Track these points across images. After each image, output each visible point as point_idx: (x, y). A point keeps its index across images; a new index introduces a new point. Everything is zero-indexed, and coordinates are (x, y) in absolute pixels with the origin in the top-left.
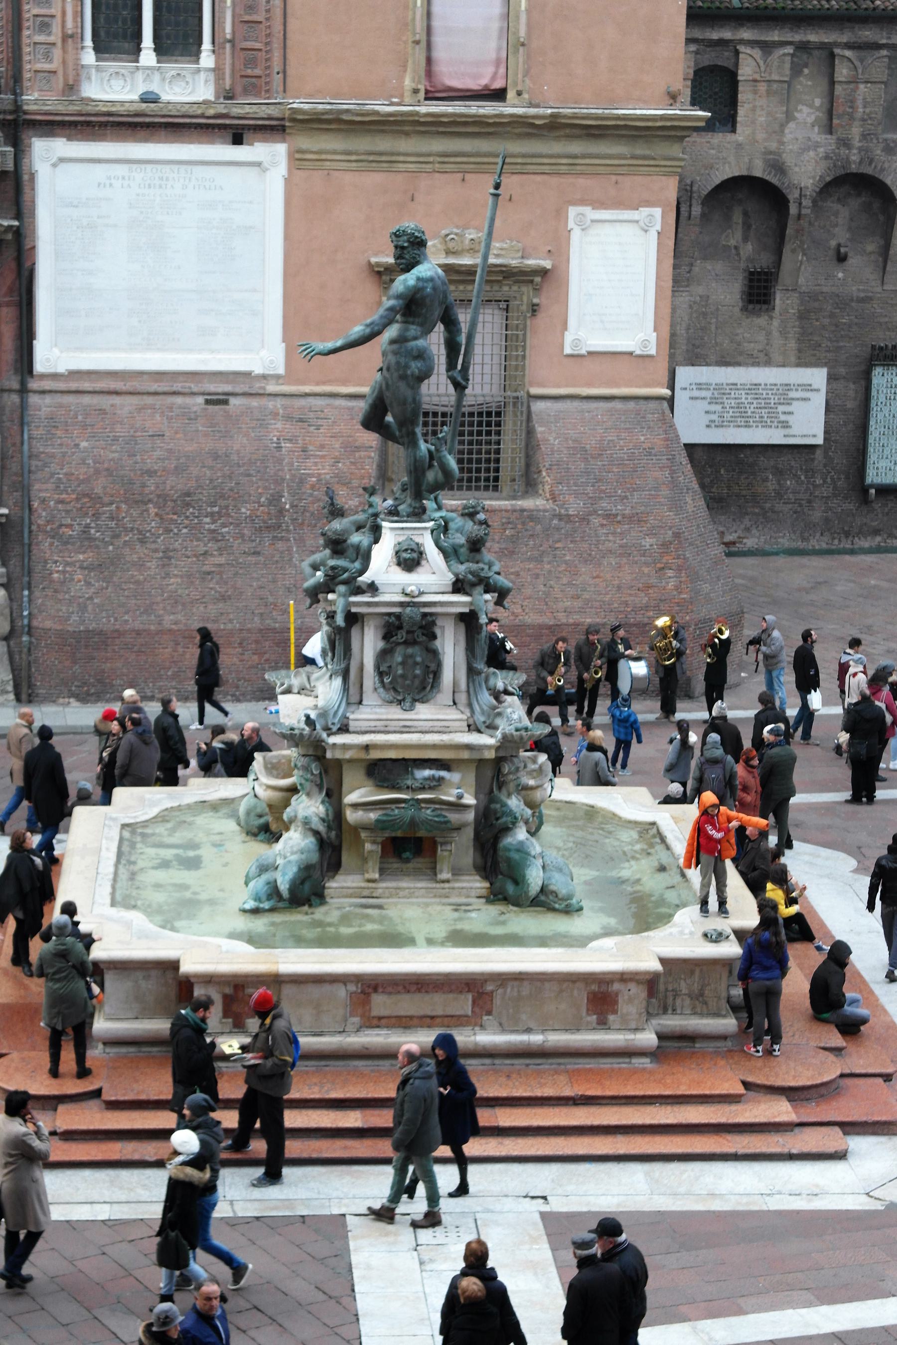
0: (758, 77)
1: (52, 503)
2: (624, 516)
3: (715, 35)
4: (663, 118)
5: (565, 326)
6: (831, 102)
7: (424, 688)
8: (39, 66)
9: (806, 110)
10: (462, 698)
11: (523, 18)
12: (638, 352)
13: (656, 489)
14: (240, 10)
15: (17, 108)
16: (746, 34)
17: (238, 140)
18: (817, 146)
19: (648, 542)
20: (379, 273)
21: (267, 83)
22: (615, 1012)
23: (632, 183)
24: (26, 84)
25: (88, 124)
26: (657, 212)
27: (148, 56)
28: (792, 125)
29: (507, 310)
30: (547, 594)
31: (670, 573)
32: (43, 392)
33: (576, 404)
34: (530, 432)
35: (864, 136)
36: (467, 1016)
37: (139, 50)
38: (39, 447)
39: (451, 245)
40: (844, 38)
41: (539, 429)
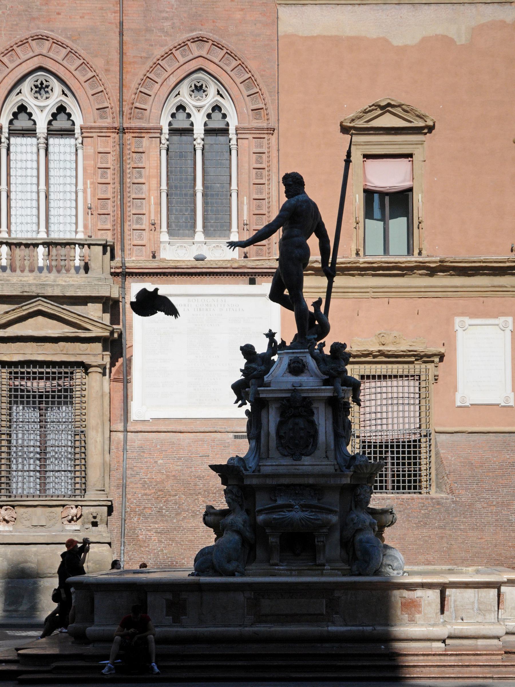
1: (140, 495)
5: (455, 389)
7: (307, 446)
8: (136, 242)
10: (331, 454)
17: (252, 282)
21: (269, 249)
22: (420, 612)
25: (165, 274)
27: (200, 236)
29: (420, 380)
36: (322, 614)
37: (195, 232)
39: (383, 340)
41: (442, 451)
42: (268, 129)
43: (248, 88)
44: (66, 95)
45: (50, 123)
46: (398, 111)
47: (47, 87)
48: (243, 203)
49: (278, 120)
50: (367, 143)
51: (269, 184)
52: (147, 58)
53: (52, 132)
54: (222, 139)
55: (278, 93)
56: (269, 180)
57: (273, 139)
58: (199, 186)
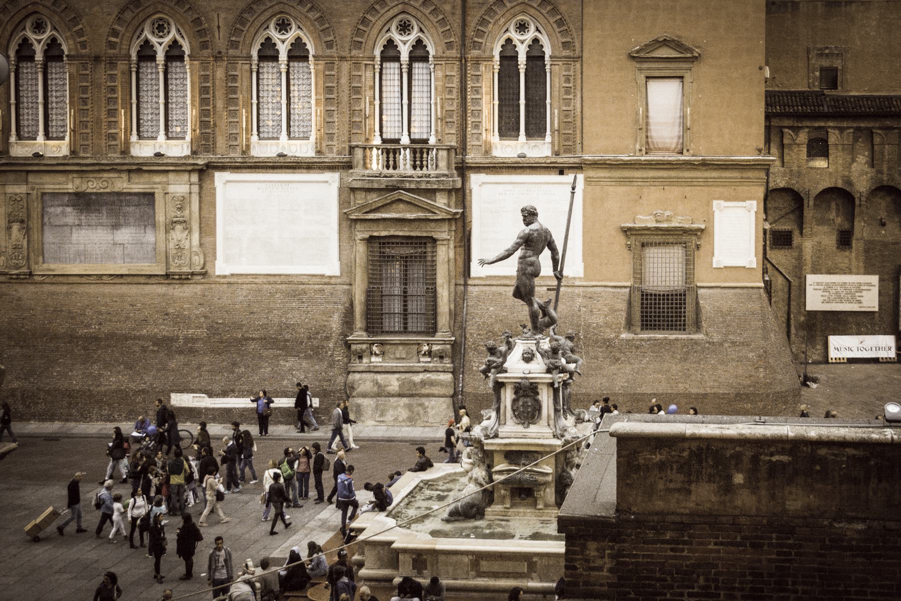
0: (837, 142)
2: (740, 343)
3: (816, 125)
4: (753, 160)
6: (873, 154)
8: (474, 143)
9: (861, 157)
11: (689, 118)
12: (747, 267)
13: (756, 330)
14: (562, 117)
15: (463, 161)
16: (831, 124)
17: (561, 173)
18: (867, 173)
19: (751, 355)
20: (625, 231)
21: (574, 148)
23: (743, 189)
24: (468, 151)
26: (754, 203)
28: (855, 164)
30: (702, 379)
31: (761, 370)
32: (475, 285)
33: (719, 290)
34: (697, 303)
35: (889, 169)
38: (471, 310)
39: (658, 218)
40: (877, 125)
41: (701, 302)
42: (573, 58)
43: (559, 26)
44: (423, 32)
45: (411, 52)
46: (672, 45)
47: (409, 25)
48: (554, 113)
49: (582, 50)
50: (649, 69)
51: (574, 100)
52: (483, 4)
53: (413, 59)
54: (539, 63)
55: (582, 29)
56: (574, 96)
57: (578, 65)
58: (522, 101)
